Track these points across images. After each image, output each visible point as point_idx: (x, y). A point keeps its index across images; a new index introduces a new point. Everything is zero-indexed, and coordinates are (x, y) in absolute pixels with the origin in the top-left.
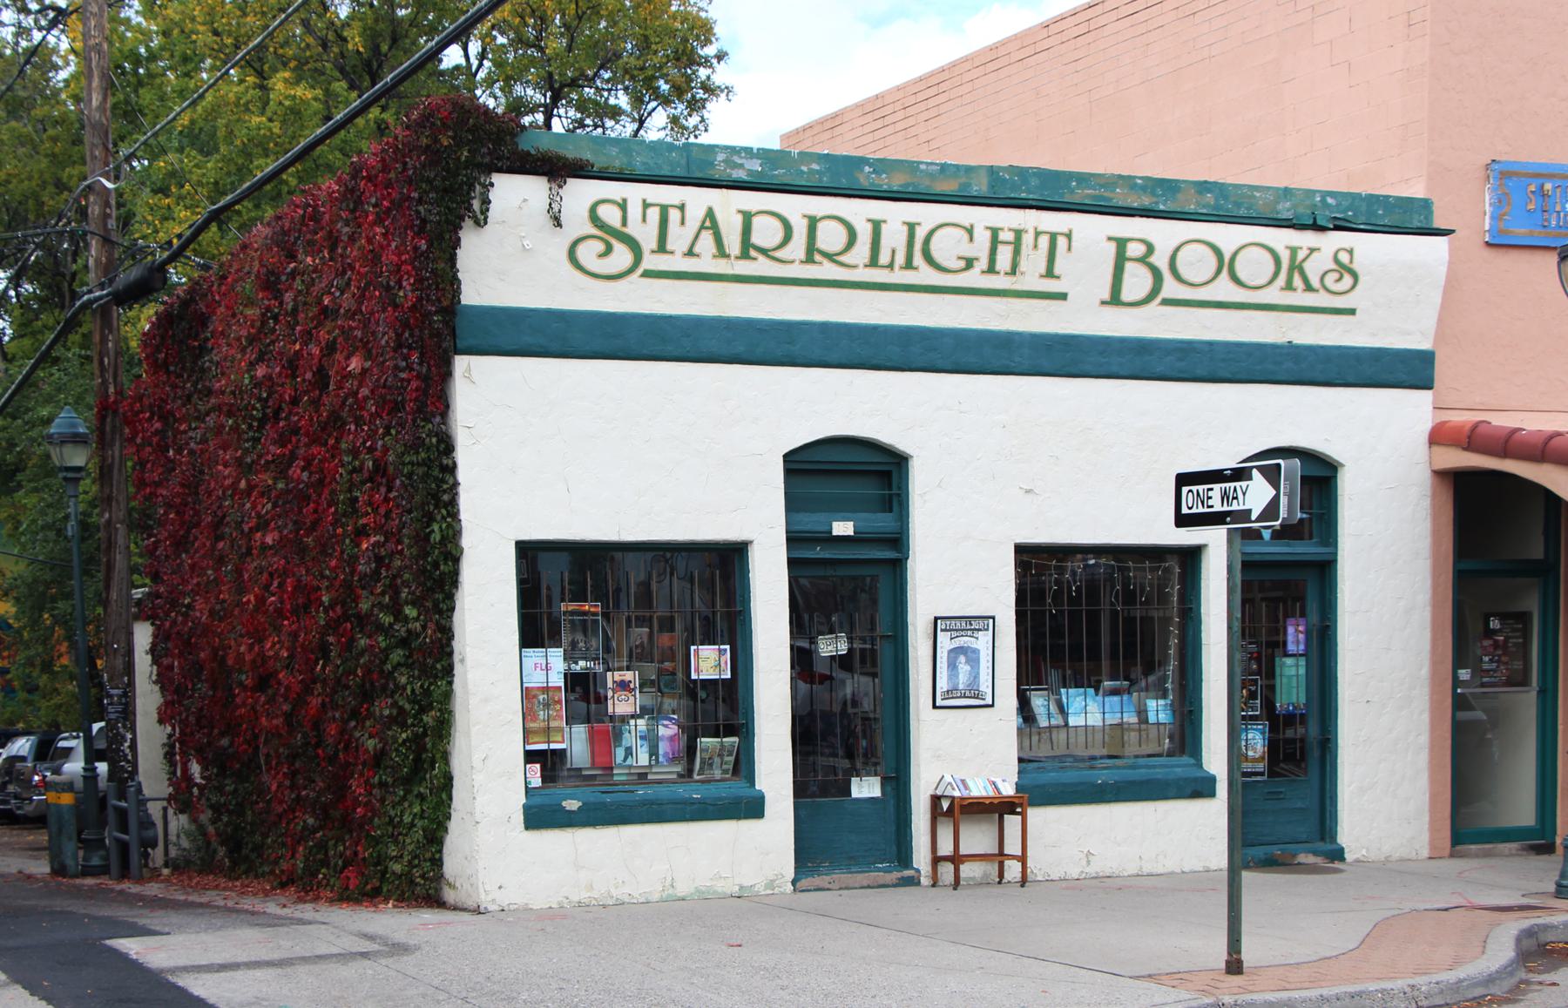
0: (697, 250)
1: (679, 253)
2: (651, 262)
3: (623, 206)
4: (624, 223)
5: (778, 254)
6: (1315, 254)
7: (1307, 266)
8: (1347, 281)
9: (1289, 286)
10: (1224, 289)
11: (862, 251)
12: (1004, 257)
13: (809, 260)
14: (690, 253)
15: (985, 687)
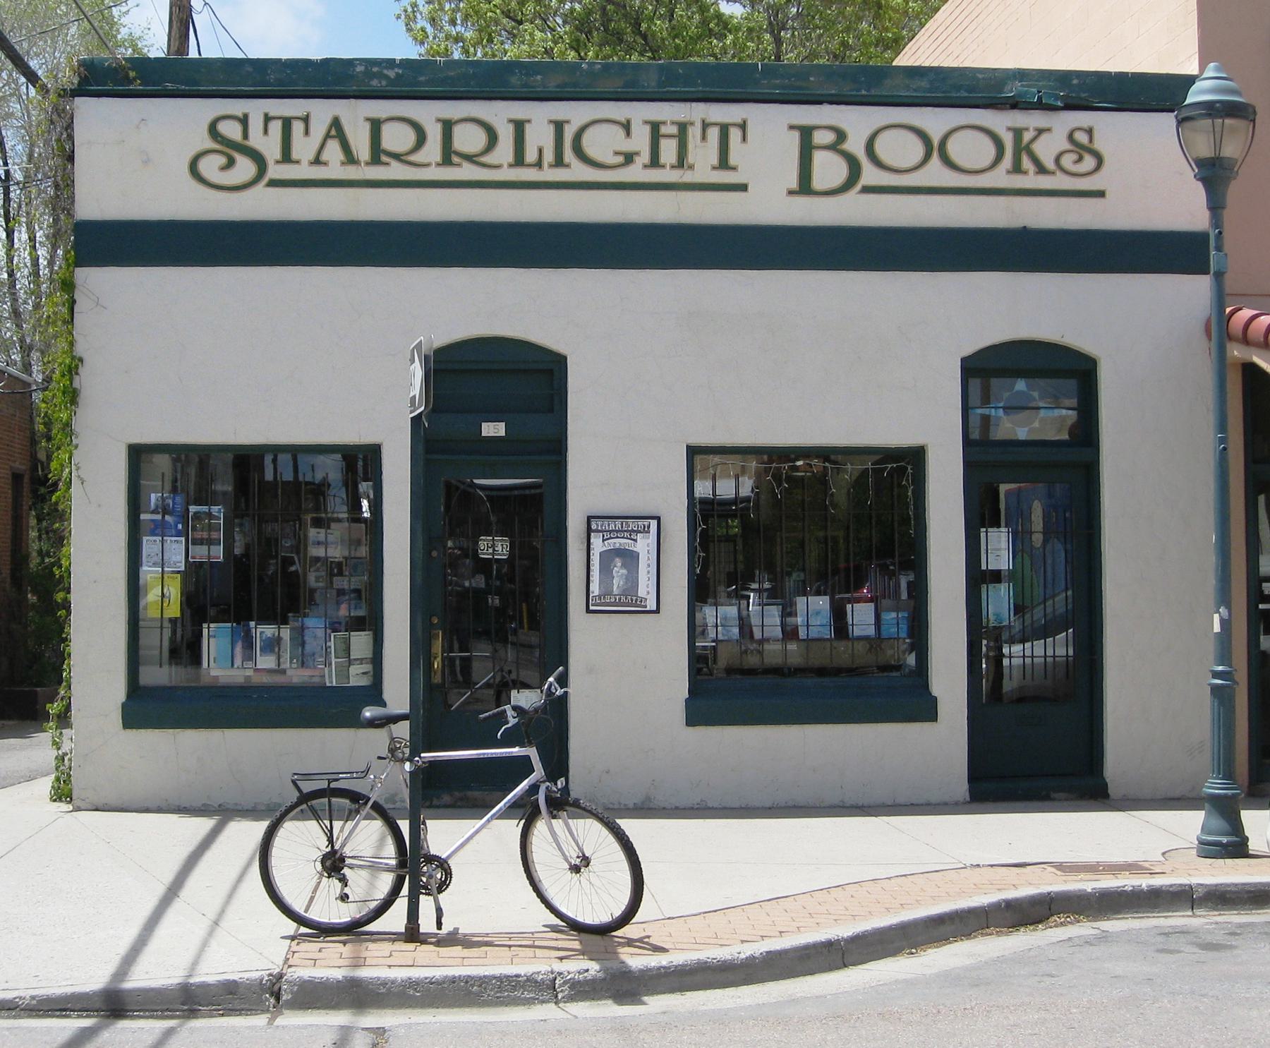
0: (324, 157)
1: (305, 163)
2: (275, 171)
3: (244, 121)
4: (246, 136)
5: (412, 158)
6: (1044, 137)
7: (1038, 148)
8: (1089, 162)
9: (1017, 169)
10: (935, 174)
11: (432, 150)
12: (668, 151)
13: (447, 160)
14: (317, 161)
15: (645, 588)
